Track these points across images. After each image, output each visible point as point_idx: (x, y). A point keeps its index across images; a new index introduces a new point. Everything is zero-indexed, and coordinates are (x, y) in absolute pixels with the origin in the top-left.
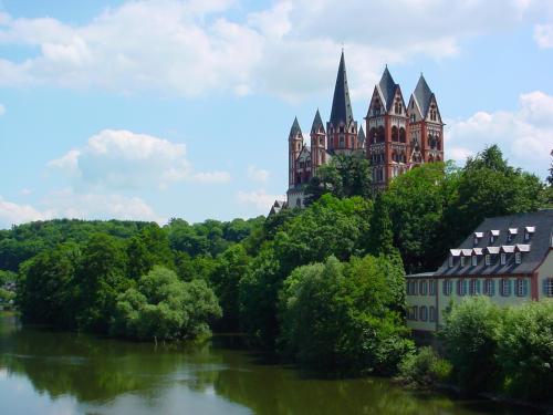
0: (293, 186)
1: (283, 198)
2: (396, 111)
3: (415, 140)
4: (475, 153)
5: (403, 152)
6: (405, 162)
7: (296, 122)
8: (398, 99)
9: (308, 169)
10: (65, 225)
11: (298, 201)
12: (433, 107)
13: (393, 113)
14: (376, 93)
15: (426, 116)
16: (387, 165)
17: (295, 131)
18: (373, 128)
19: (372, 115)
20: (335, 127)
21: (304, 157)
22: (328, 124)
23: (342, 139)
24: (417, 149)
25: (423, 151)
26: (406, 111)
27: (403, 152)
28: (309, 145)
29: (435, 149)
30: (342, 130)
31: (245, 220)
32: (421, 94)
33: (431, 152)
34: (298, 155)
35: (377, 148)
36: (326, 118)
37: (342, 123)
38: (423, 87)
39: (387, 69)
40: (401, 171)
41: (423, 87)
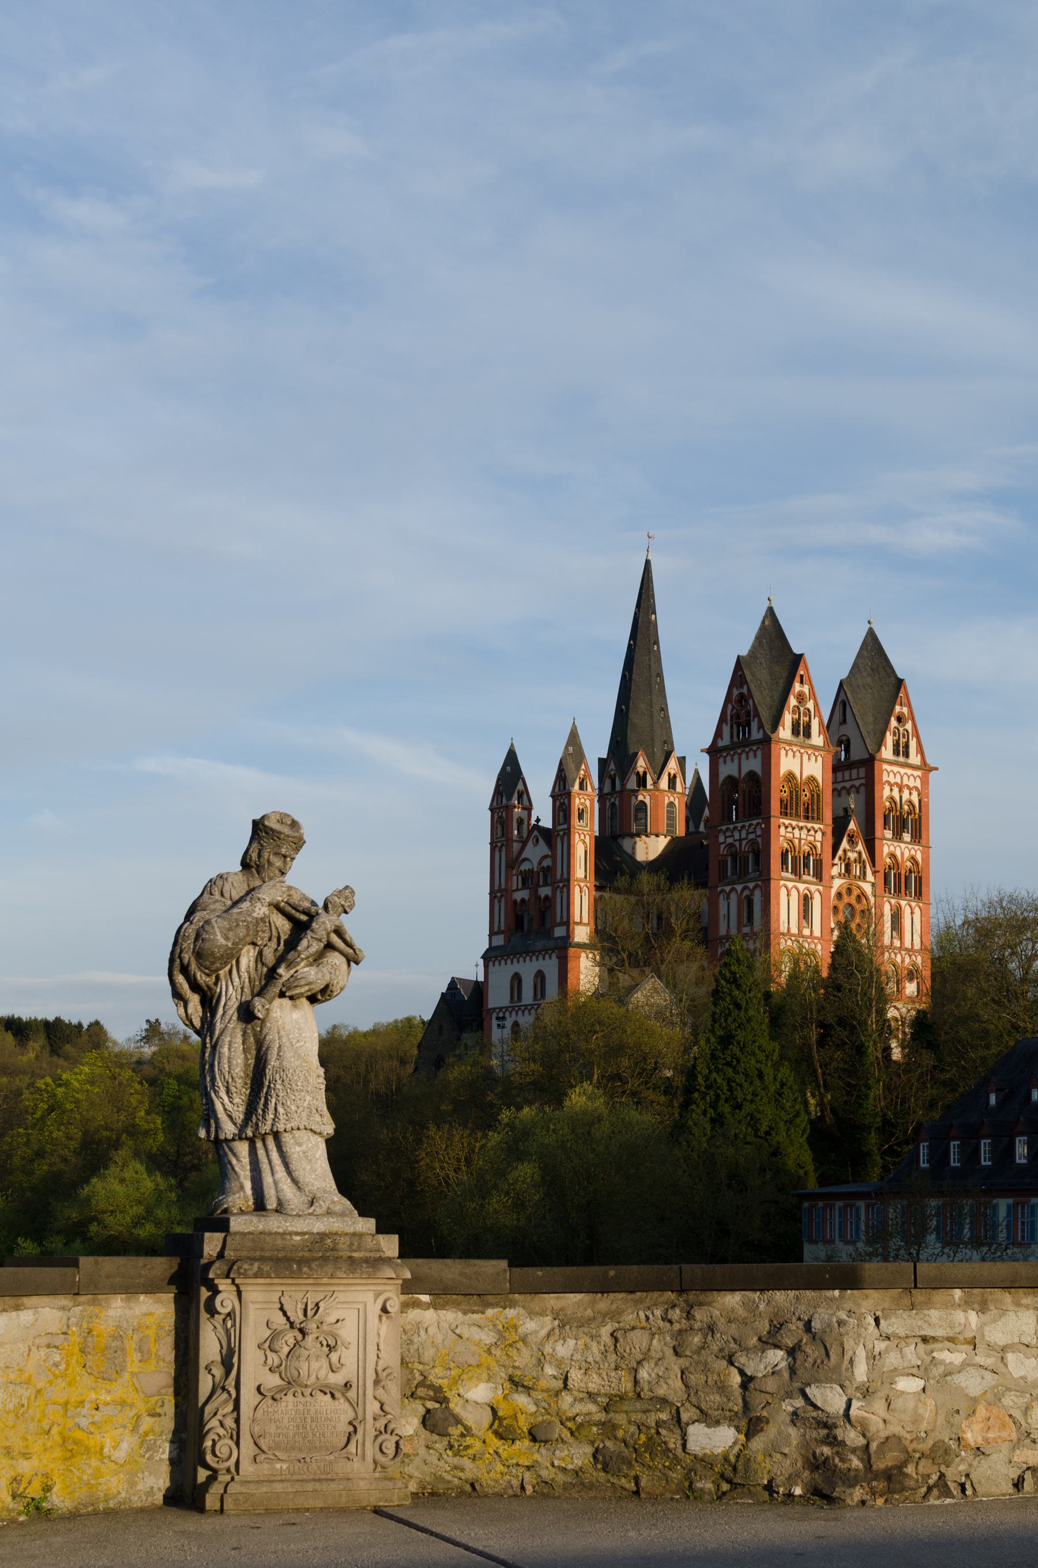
0: (499, 940)
2: (795, 731)
6: (819, 875)
7: (512, 758)
8: (801, 698)
9: (544, 891)
11: (517, 978)
13: (785, 732)
15: (880, 742)
16: (767, 881)
17: (510, 779)
18: (730, 778)
19: (725, 741)
21: (535, 853)
22: (601, 761)
28: (547, 823)
29: (907, 837)
33: (894, 848)
34: (516, 847)
35: (734, 836)
36: (597, 746)
39: (771, 611)
40: (806, 901)
41: (872, 650)
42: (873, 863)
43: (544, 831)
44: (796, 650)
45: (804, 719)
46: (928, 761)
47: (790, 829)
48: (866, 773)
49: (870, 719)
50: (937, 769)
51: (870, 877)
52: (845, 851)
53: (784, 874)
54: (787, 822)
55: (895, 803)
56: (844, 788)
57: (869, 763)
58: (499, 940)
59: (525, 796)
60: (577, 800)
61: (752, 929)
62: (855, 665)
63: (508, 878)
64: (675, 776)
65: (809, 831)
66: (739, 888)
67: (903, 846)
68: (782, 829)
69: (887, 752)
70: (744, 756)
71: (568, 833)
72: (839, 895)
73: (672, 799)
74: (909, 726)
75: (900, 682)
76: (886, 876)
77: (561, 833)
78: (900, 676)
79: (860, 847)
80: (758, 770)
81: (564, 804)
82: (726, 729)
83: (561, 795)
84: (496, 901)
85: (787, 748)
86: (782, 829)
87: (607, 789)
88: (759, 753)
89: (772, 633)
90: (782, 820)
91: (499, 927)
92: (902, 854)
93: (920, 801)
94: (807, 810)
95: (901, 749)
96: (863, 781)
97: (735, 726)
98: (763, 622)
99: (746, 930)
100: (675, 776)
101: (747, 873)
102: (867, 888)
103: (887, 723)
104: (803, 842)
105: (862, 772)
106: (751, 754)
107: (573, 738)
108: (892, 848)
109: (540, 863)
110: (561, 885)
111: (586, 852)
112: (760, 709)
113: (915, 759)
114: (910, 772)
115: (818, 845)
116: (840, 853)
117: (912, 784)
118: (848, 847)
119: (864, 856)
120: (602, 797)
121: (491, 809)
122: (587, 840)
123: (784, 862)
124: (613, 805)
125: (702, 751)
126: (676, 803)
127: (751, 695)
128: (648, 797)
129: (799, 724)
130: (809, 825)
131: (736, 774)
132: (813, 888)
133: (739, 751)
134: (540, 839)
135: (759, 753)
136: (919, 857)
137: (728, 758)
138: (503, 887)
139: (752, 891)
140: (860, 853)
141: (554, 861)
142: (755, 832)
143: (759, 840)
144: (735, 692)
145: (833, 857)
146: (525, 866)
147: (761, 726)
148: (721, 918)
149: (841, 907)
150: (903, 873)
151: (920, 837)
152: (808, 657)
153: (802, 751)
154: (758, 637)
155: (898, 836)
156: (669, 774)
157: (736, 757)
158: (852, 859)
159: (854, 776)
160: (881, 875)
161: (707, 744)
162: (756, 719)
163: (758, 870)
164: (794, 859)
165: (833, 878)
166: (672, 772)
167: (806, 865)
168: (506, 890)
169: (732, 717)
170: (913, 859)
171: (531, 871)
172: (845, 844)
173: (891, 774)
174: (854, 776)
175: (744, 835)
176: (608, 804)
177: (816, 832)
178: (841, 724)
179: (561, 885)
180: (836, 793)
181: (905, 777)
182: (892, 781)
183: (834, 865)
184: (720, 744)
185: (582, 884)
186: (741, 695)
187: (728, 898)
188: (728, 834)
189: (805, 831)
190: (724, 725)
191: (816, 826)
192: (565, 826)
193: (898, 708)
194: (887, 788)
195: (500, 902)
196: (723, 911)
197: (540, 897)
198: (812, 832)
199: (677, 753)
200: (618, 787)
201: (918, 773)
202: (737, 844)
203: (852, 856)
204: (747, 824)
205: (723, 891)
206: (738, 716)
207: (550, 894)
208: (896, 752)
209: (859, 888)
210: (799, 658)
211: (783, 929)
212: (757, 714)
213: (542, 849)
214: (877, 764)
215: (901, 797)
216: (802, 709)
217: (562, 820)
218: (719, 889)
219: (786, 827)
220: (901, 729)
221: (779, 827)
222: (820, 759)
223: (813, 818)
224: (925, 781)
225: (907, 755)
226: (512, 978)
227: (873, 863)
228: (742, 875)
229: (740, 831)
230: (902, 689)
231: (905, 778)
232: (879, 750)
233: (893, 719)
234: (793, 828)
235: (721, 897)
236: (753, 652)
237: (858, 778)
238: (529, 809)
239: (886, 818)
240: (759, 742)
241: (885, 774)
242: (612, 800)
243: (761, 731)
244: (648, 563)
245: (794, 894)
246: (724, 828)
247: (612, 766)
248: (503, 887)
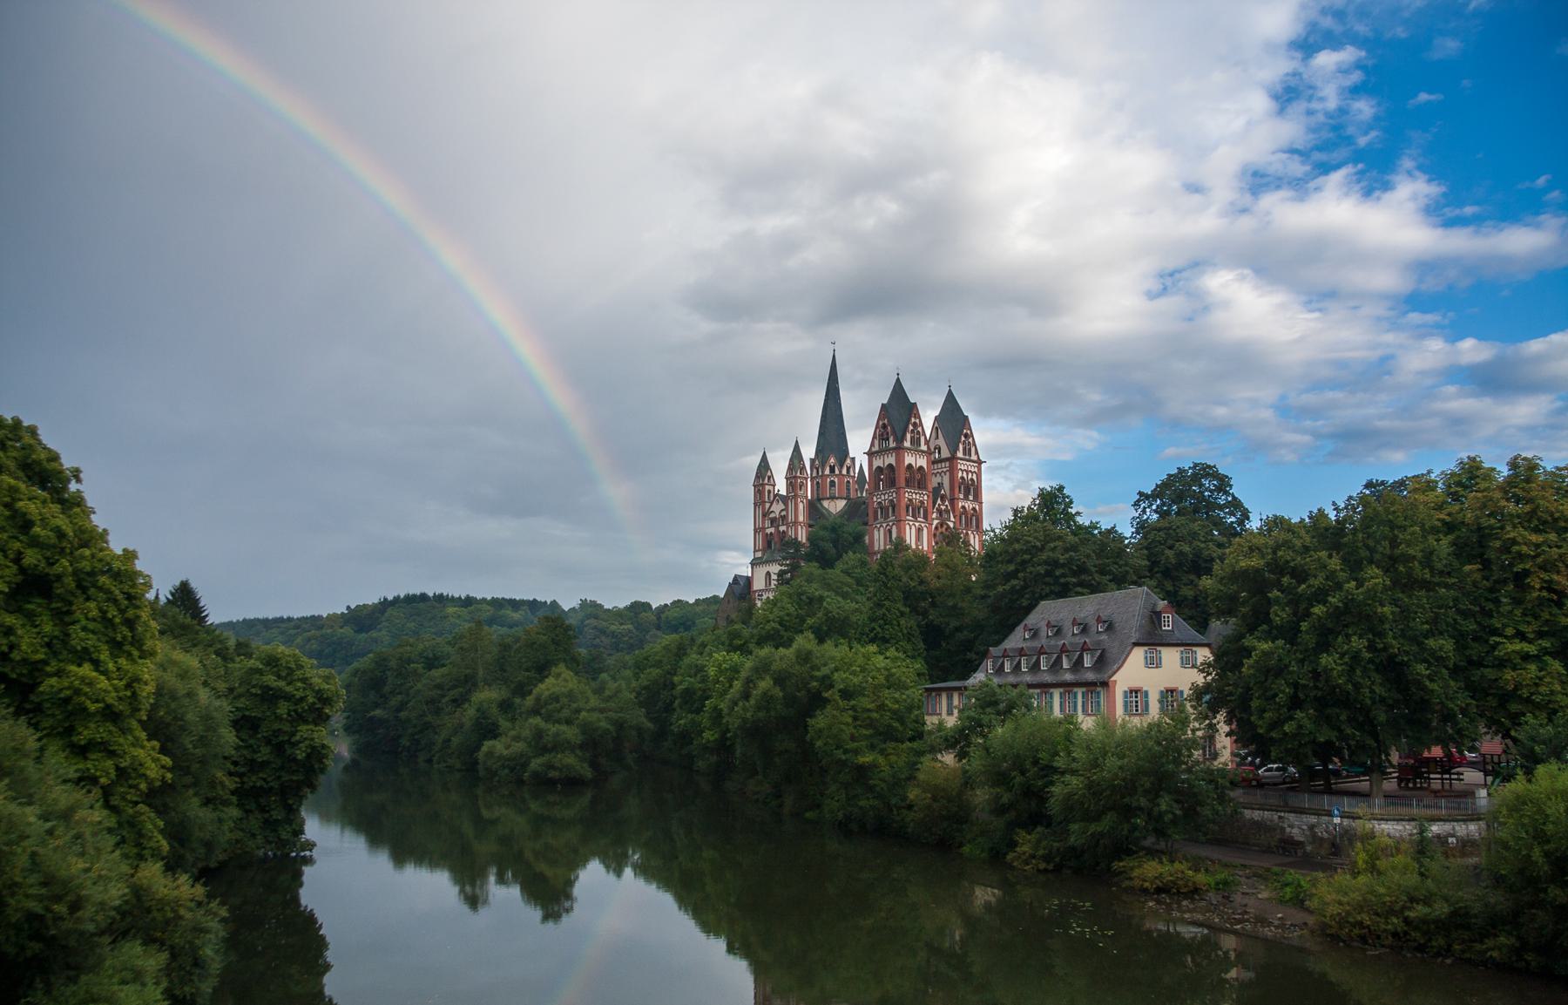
3: (940, 485)
4: (1026, 498)
6: (925, 517)
9: (782, 528)
10: (421, 605)
11: (768, 574)
13: (907, 444)
16: (899, 522)
19: (876, 448)
20: (823, 465)
21: (777, 508)
22: (812, 461)
23: (832, 483)
24: (943, 498)
25: (953, 501)
26: (927, 442)
28: (783, 492)
30: (832, 470)
31: (692, 601)
35: (883, 498)
36: (809, 452)
40: (919, 530)
57: (952, 459)
58: (759, 554)
69: (960, 454)
71: (795, 497)
89: (898, 391)
95: (967, 452)
107: (797, 449)
113: (974, 457)
155: (966, 497)
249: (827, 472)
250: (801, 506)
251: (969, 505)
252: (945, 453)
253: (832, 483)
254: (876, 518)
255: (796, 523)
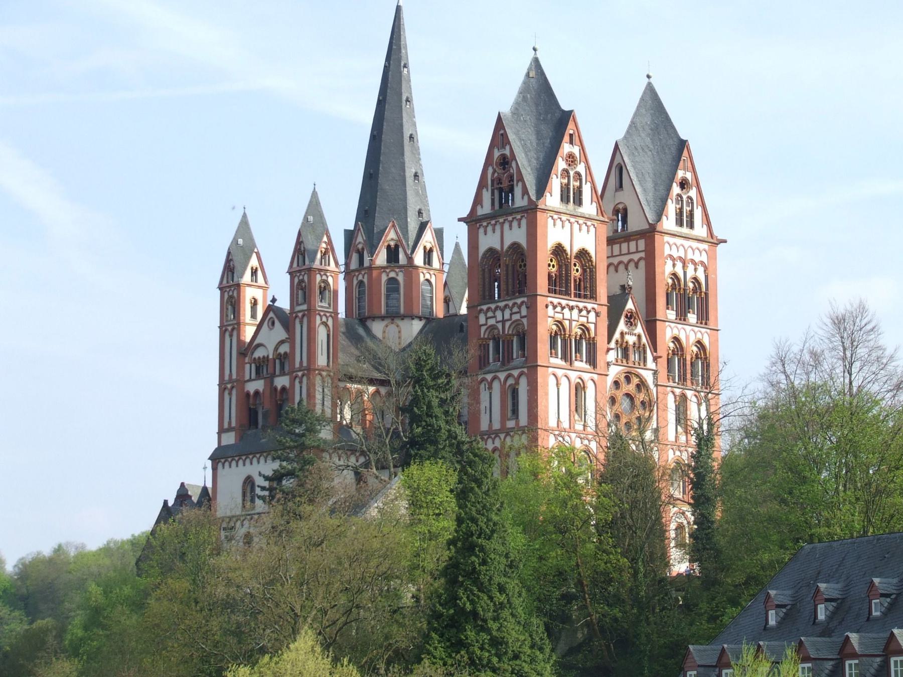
0: (230, 439)
1: (199, 476)
2: (565, 198)
3: (625, 290)
5: (585, 328)
6: (592, 360)
9: (281, 382)
11: (249, 482)
12: (684, 184)
13: (552, 199)
14: (500, 136)
15: (660, 213)
16: (531, 368)
18: (491, 250)
19: (486, 208)
22: (350, 236)
23: (392, 281)
24: (631, 319)
25: (651, 326)
26: (600, 198)
27: (585, 328)
28: (284, 303)
29: (692, 318)
30: (393, 254)
32: (644, 139)
35: (499, 317)
36: (341, 216)
37: (391, 236)
38: (653, 112)
39: (536, 62)
40: (579, 389)
42: (655, 348)
43: (279, 312)
44: (565, 106)
45: (574, 184)
46: (715, 233)
47: (559, 309)
48: (646, 245)
49: (650, 185)
50: (725, 241)
51: (651, 364)
52: (622, 334)
53: (553, 361)
54: (556, 301)
55: (679, 280)
56: (620, 262)
57: (650, 234)
58: (230, 439)
59: (259, 273)
60: (318, 278)
61: (517, 424)
62: (633, 124)
63: (241, 368)
64: (431, 250)
65: (580, 311)
66: (502, 376)
67: (688, 328)
68: (550, 307)
69: (669, 223)
70: (506, 226)
71: (310, 313)
72: (616, 384)
73: (428, 276)
74: (693, 193)
75: (682, 145)
76: (669, 362)
77: (300, 315)
78: (683, 137)
79: (639, 329)
80: (524, 243)
81: (302, 281)
82: (487, 196)
83: (300, 271)
84: (226, 392)
85: (555, 217)
86: (550, 307)
87: (354, 265)
88: (524, 222)
90: (550, 299)
91: (230, 423)
92: (687, 337)
93: (707, 277)
94: (578, 287)
95: (685, 219)
96: (643, 255)
97: (496, 193)
98: (528, 75)
99: (511, 424)
100: (431, 250)
101: (510, 358)
102: (648, 376)
103: (669, 189)
104: (574, 323)
105: (642, 244)
106: (515, 224)
107: (314, 206)
108: (676, 332)
109: (276, 349)
110: (300, 374)
111: (328, 336)
112: (523, 171)
113: (700, 230)
114: (695, 244)
115: (592, 327)
116: (617, 335)
117: (697, 259)
118: (625, 330)
119: (644, 340)
120: (348, 274)
121: (221, 288)
122: (330, 323)
123: (553, 345)
124: (361, 283)
125: (460, 220)
126: (433, 280)
127: (514, 157)
128: (401, 274)
129: (568, 189)
130: (581, 305)
131: (498, 247)
132: (586, 377)
133: (501, 220)
134: (277, 323)
135: (524, 222)
136: (706, 342)
137: (490, 228)
138: (234, 377)
139: (517, 382)
140: (639, 337)
141: (293, 347)
142: (519, 312)
143: (525, 321)
144: (497, 154)
145: (609, 342)
146: (259, 353)
147: (525, 192)
148: (483, 412)
149: (619, 394)
150: (688, 358)
151: (707, 319)
152: (579, 116)
153: (572, 220)
154: (524, 91)
155: (682, 316)
156: (425, 248)
157: (498, 227)
158: (631, 343)
159: (633, 249)
160: (663, 362)
161: (465, 213)
162: (520, 184)
163: (524, 356)
164: (564, 341)
165: (608, 364)
166: (428, 246)
167: (578, 350)
168: (237, 381)
169: (492, 181)
170: (699, 343)
171: (266, 359)
172: (622, 326)
173: (674, 247)
174: (633, 249)
175: (507, 316)
176: (355, 282)
177: (588, 312)
178: (616, 190)
179: (300, 374)
180: (612, 269)
181: (690, 251)
182: (675, 255)
183: (609, 350)
184: (480, 212)
185: (324, 373)
186: (503, 157)
187: (490, 388)
188: (490, 314)
189: (575, 311)
190: (484, 190)
191: (589, 306)
192: (304, 307)
193: (680, 174)
194: (669, 263)
195: (230, 394)
196: (484, 403)
197: (276, 389)
198: (584, 313)
199: (435, 223)
200: (366, 264)
201: (705, 246)
202: (500, 326)
203: (631, 339)
204: (510, 303)
205: (483, 380)
206: (500, 181)
207: (287, 385)
208: (680, 222)
209: (638, 376)
210: (566, 117)
211: (552, 423)
212: (521, 179)
213: (279, 333)
214: (657, 237)
215: (685, 273)
216: (572, 173)
217: (300, 300)
218: (480, 377)
219: (555, 307)
220: (685, 197)
221: (547, 306)
222: (592, 229)
223: (585, 297)
224: (712, 257)
225: (691, 225)
226: (245, 483)
227: (655, 348)
228: (506, 360)
229: (503, 311)
230: (685, 152)
231: (690, 251)
232: (659, 219)
233: (674, 185)
234: (563, 308)
235: (482, 386)
236: (516, 111)
237: (637, 252)
238: (265, 289)
239: (668, 296)
240: (523, 210)
241: (667, 247)
242: (360, 277)
243: (526, 197)
244: (398, 9)
245: (564, 383)
246: (485, 307)
247: (360, 239)
248: (234, 377)
249: (381, 258)
250: (322, 334)
251: (690, 333)
252: (635, 224)
253: (392, 281)
254: (483, 362)
255: (309, 369)
